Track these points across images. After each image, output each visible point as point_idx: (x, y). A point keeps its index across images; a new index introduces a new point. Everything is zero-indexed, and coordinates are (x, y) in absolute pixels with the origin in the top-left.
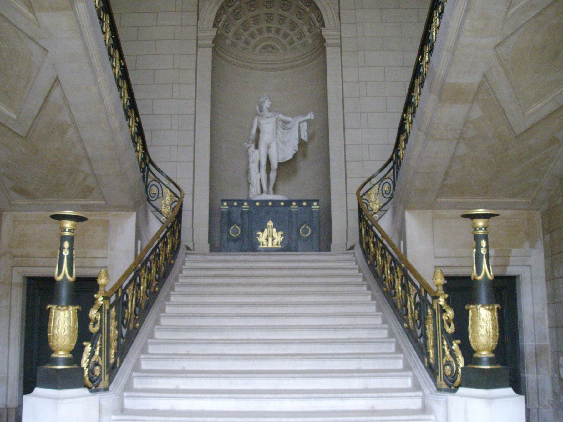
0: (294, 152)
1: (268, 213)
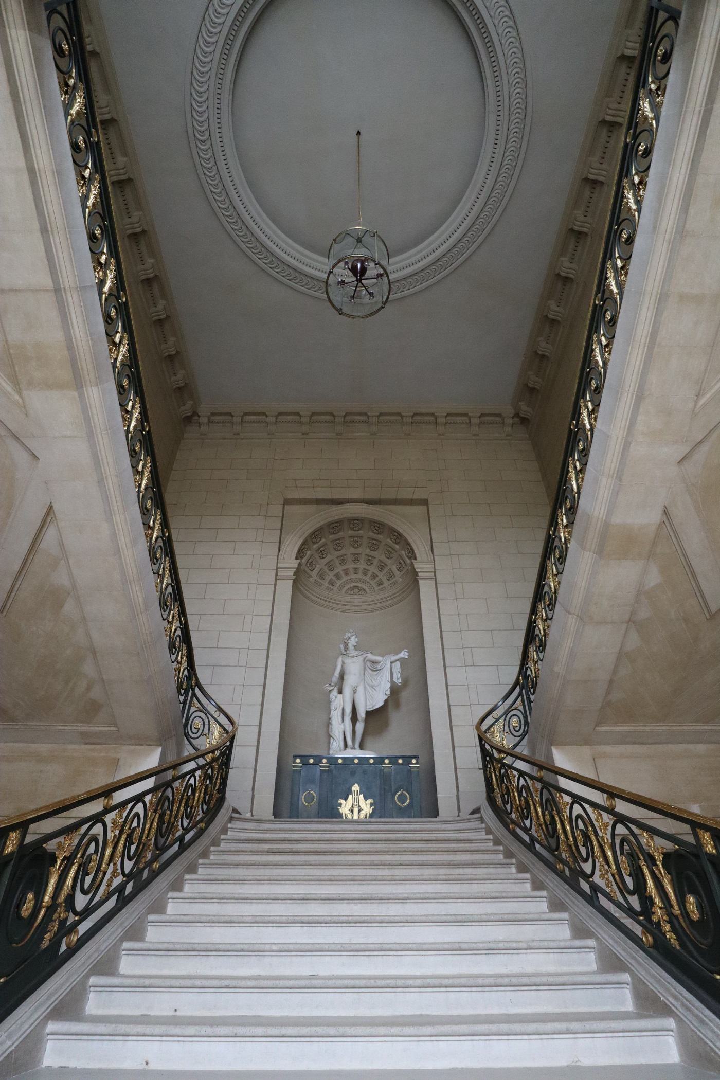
0: (386, 697)
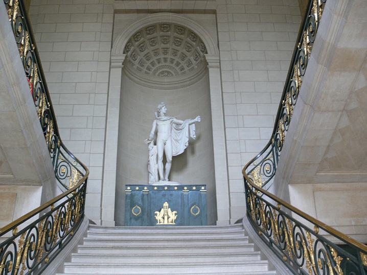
0: (186, 147)
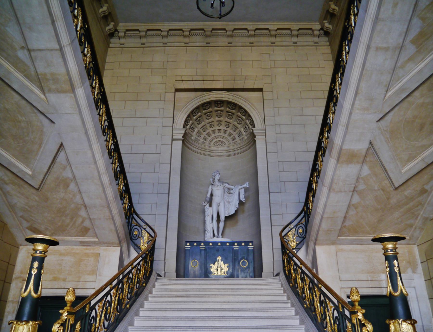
0: (236, 209)
1: (218, 251)
